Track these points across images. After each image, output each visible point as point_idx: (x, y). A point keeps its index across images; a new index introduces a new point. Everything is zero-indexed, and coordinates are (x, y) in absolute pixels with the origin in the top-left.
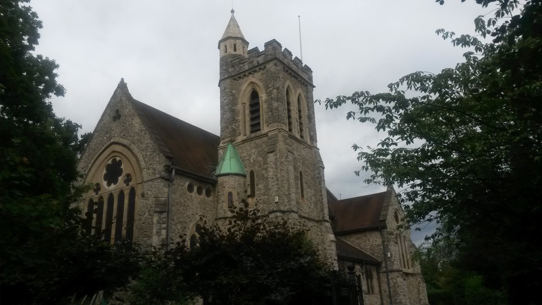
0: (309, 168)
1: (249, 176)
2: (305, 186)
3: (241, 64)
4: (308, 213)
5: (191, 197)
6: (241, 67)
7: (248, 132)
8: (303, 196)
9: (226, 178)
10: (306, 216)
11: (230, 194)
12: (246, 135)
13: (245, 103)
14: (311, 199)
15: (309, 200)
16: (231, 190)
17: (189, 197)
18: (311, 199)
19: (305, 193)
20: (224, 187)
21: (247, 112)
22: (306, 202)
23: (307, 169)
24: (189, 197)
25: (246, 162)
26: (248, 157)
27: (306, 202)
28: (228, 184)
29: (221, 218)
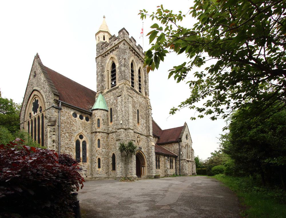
2: (140, 117)
3: (106, 47)
6: (106, 49)
8: (138, 122)
9: (97, 111)
10: (140, 133)
11: (99, 120)
14: (143, 124)
17: (74, 120)
18: (143, 124)
20: (95, 116)
24: (74, 120)
29: (94, 132)
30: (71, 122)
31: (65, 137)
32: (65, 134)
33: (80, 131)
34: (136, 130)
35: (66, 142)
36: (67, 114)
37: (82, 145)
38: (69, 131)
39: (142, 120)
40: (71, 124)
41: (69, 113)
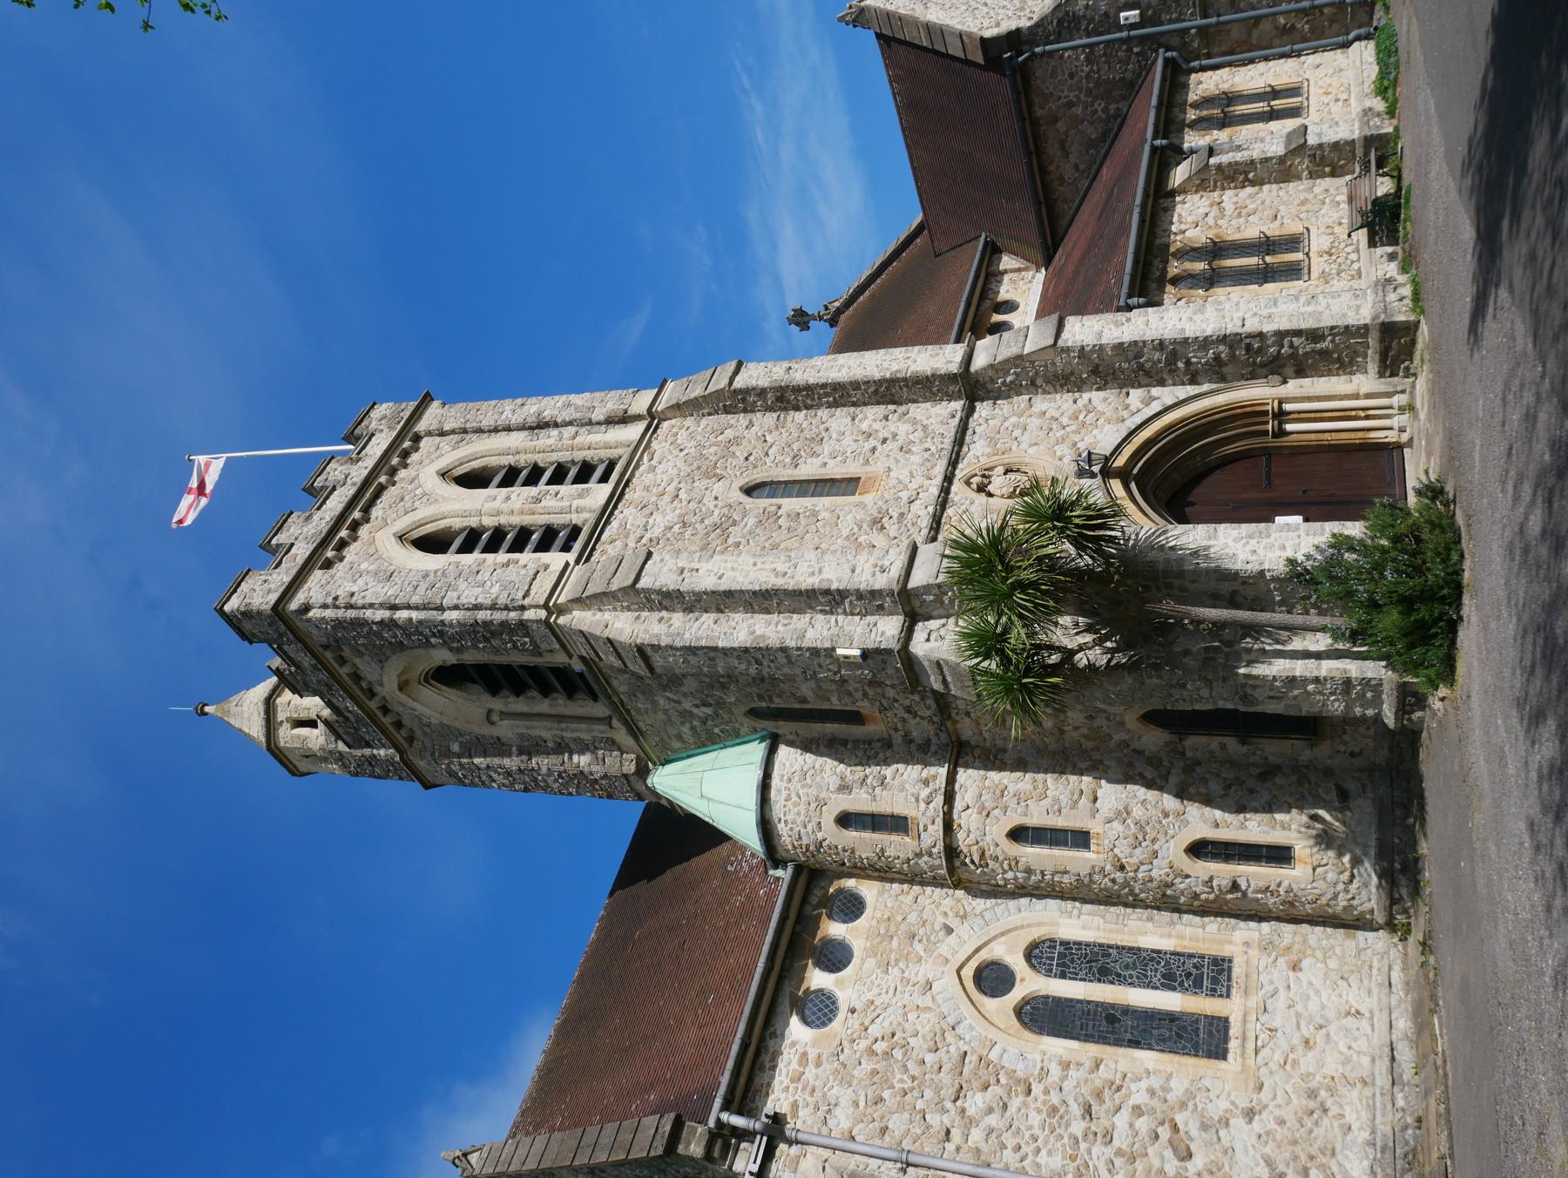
0: (736, 441)
1: (773, 723)
4: (926, 455)
5: (853, 1011)
7: (600, 710)
8: (849, 485)
12: (610, 718)
13: (490, 712)
15: (874, 450)
16: (828, 819)
17: (854, 1022)
19: (835, 470)
21: (519, 705)
22: (878, 467)
23: (740, 453)
24: (854, 1022)
25: (716, 730)
26: (696, 723)
27: (878, 467)
28: (805, 827)
30: (871, 1052)
31: (993, 1120)
32: (969, 1123)
33: (946, 984)
34: (916, 506)
35: (1035, 1119)
36: (810, 1072)
37: (1063, 976)
38: (945, 1078)
39: (827, 448)
40: (888, 1054)
41: (805, 1054)
